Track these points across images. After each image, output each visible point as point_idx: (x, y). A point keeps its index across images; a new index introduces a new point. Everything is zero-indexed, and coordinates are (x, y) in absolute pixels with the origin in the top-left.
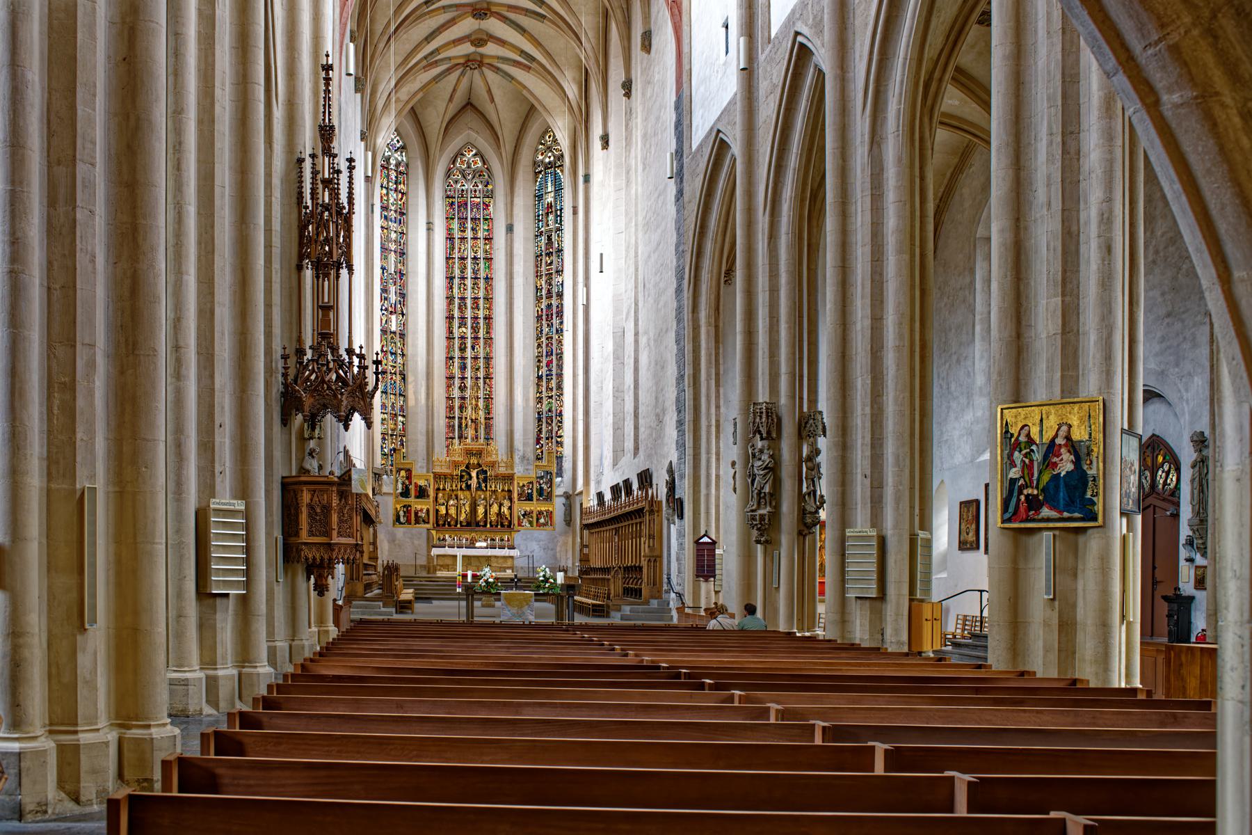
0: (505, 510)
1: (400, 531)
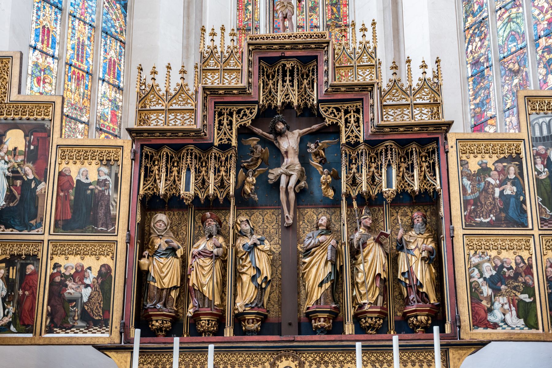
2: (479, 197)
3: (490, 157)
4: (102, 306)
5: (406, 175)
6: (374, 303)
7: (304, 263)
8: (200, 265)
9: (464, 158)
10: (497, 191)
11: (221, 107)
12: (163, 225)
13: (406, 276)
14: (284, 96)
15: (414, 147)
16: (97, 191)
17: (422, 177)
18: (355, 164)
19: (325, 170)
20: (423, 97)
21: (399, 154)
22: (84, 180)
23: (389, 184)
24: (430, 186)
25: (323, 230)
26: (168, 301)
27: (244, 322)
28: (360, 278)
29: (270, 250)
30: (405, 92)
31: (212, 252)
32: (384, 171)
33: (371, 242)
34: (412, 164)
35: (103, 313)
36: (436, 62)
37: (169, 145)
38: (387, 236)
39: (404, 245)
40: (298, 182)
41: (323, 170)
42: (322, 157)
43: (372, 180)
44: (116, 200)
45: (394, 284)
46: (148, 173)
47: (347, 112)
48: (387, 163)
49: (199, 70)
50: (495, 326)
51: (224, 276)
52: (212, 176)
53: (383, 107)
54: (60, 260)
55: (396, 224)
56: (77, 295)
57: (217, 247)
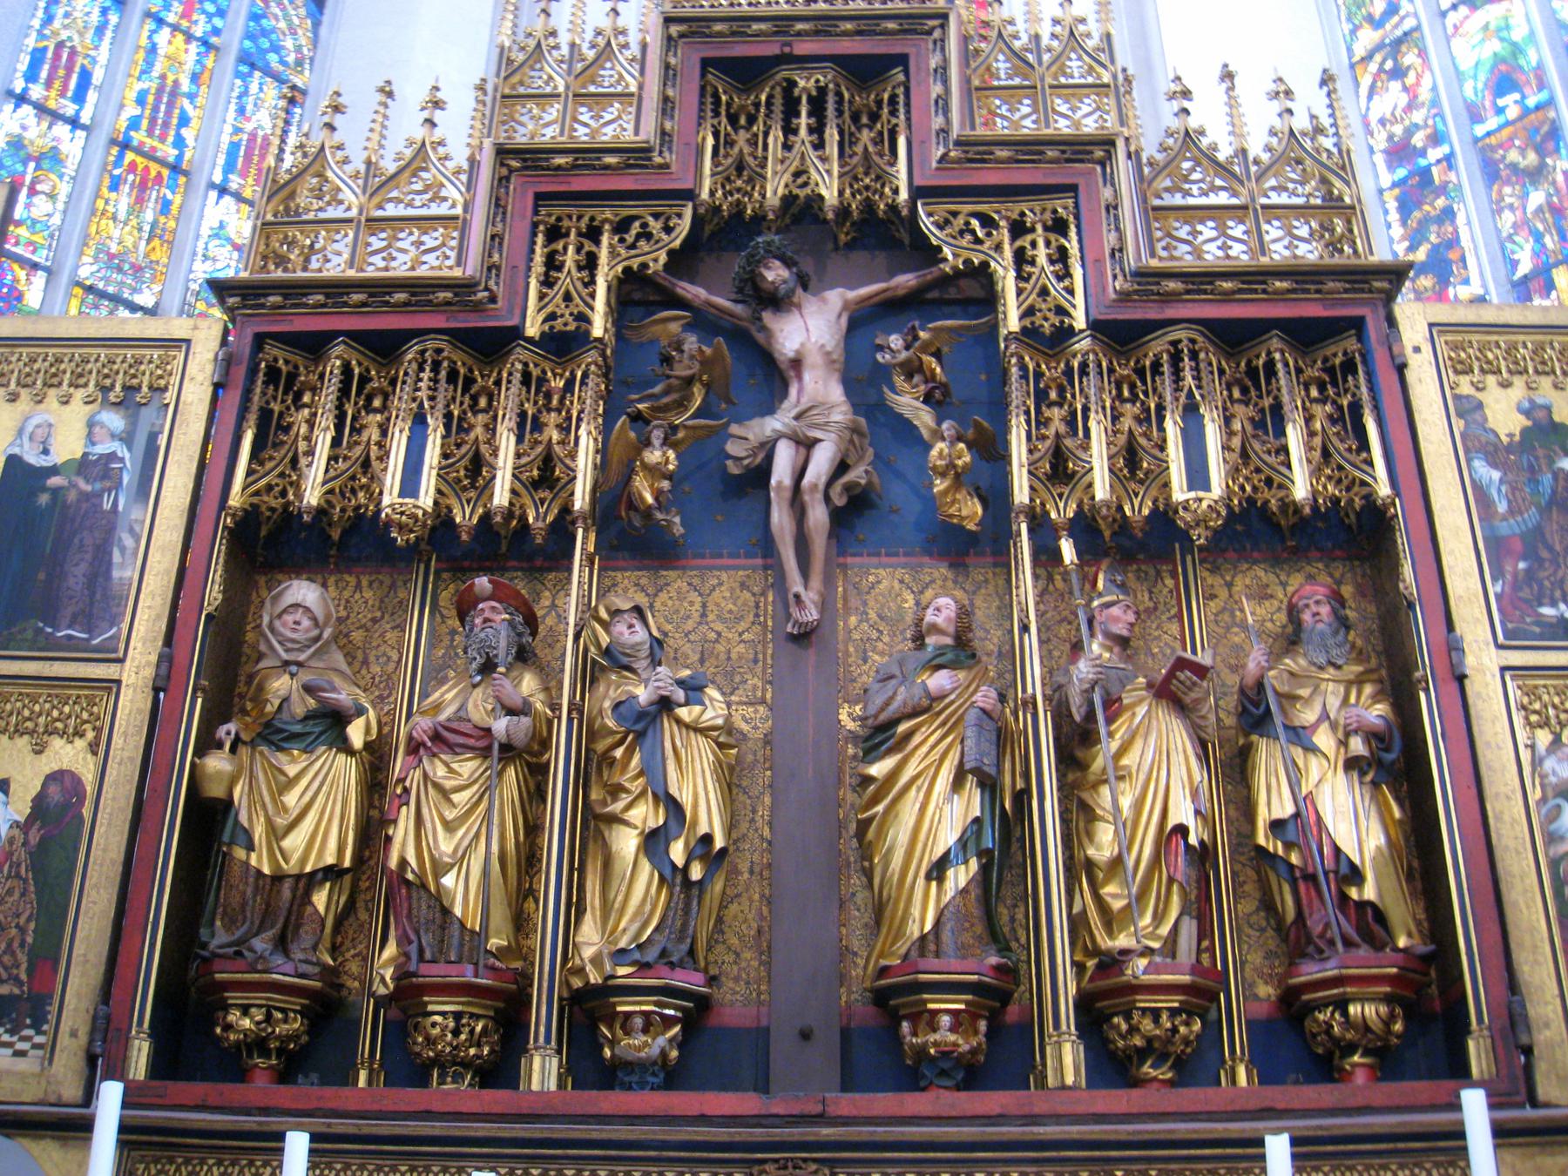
2: (1538, 531)
3: (1556, 386)
4: (30, 940)
5: (1257, 446)
6: (1160, 952)
7: (869, 780)
8: (436, 786)
9: (1465, 388)
11: (557, 211)
12: (306, 623)
13: (1291, 834)
14: (787, 177)
15: (1276, 348)
16: (72, 496)
17: (1317, 454)
18: (1061, 405)
19: (945, 426)
20: (1291, 186)
21: (1221, 372)
22: (33, 458)
23: (1200, 470)
24: (1348, 489)
25: (941, 650)
26: (298, 926)
27: (611, 1027)
28: (1103, 844)
29: (728, 728)
30: (1223, 169)
31: (488, 731)
34: (1277, 409)
35: (30, 972)
36: (1323, 83)
37: (356, 337)
38: (1201, 671)
39: (1273, 708)
40: (842, 467)
41: (939, 423)
42: (930, 378)
43: (1132, 461)
44: (137, 528)
45: (1238, 867)
46: (271, 432)
48: (1183, 400)
49: (488, 99)
51: (533, 829)
52: (507, 442)
55: (1228, 629)
57: (511, 712)
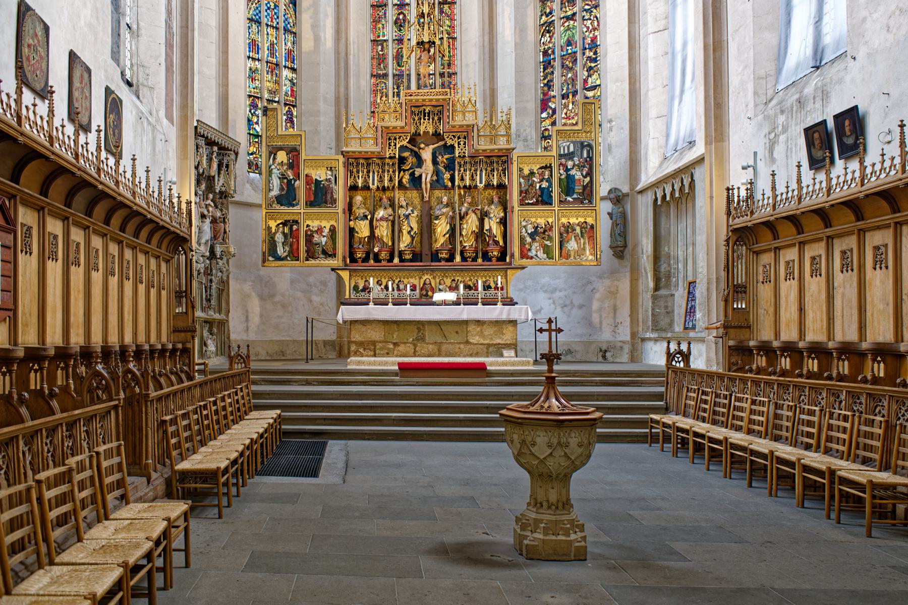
0: (493, 225)
1: (283, 275)
10: (538, 185)
32: (478, 173)
33: (470, 212)
43: (472, 178)
46: (352, 172)
47: (459, 138)
50: (532, 258)
53: (479, 136)
54: (308, 222)
56: (319, 241)
